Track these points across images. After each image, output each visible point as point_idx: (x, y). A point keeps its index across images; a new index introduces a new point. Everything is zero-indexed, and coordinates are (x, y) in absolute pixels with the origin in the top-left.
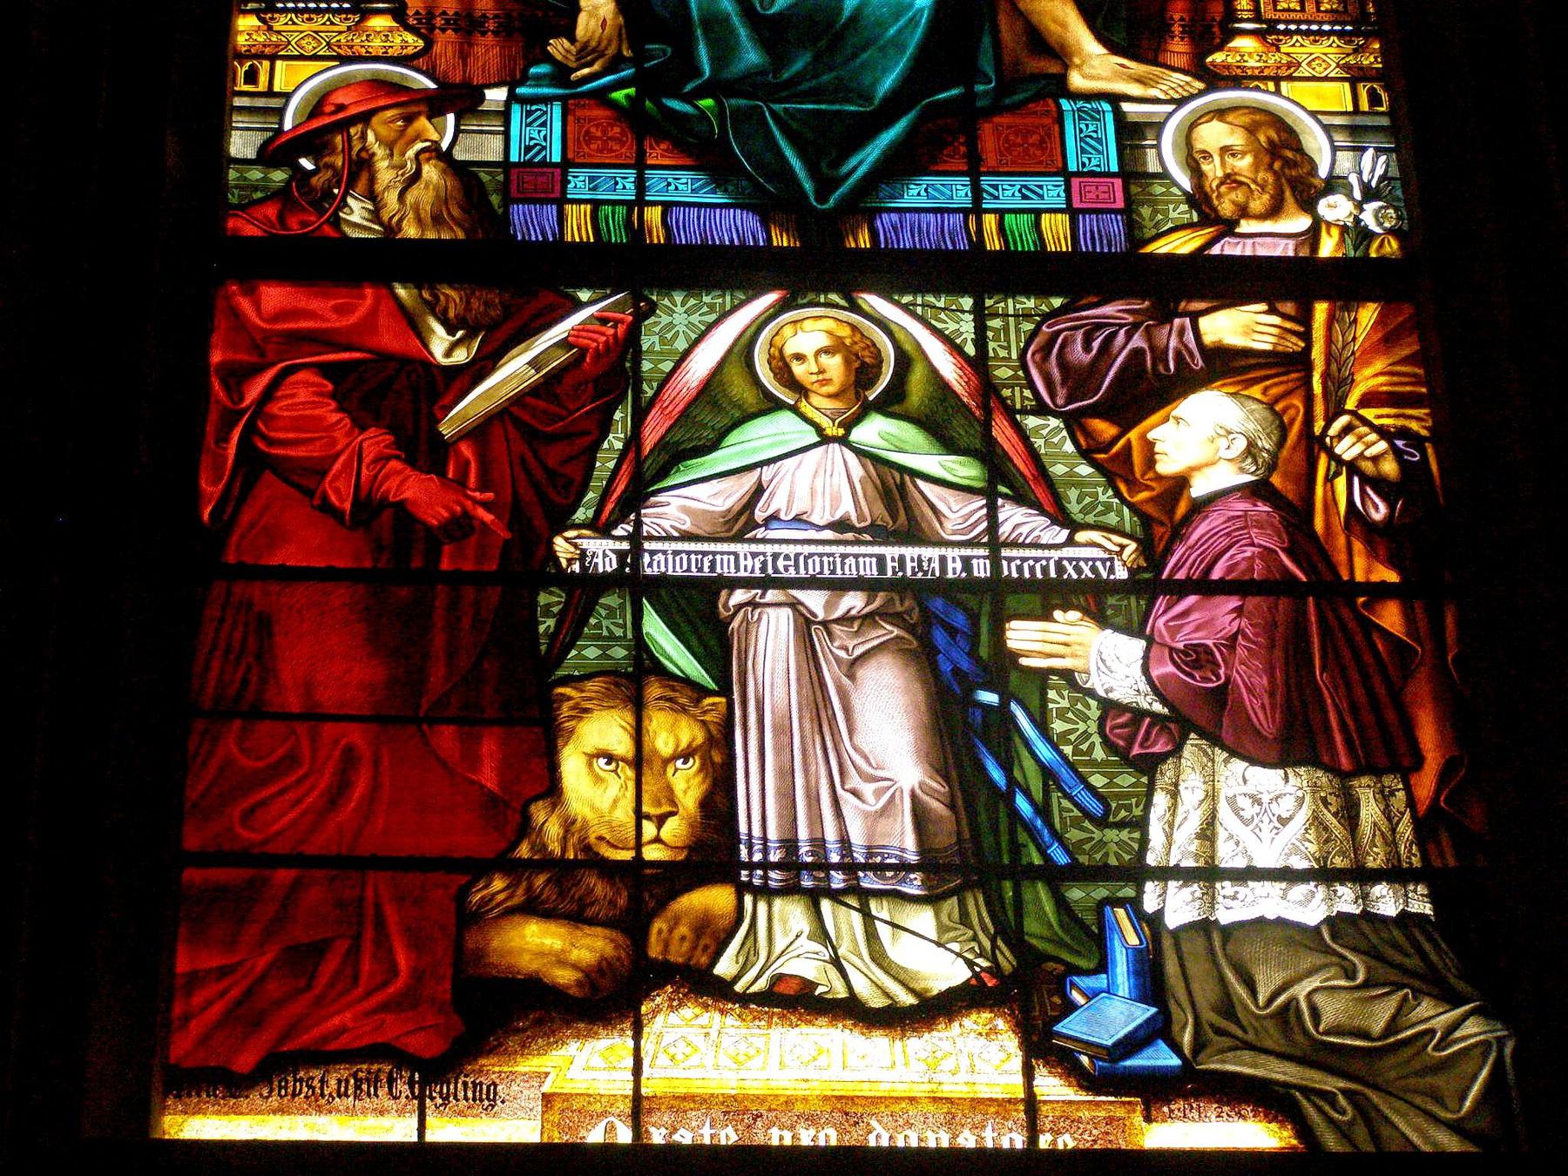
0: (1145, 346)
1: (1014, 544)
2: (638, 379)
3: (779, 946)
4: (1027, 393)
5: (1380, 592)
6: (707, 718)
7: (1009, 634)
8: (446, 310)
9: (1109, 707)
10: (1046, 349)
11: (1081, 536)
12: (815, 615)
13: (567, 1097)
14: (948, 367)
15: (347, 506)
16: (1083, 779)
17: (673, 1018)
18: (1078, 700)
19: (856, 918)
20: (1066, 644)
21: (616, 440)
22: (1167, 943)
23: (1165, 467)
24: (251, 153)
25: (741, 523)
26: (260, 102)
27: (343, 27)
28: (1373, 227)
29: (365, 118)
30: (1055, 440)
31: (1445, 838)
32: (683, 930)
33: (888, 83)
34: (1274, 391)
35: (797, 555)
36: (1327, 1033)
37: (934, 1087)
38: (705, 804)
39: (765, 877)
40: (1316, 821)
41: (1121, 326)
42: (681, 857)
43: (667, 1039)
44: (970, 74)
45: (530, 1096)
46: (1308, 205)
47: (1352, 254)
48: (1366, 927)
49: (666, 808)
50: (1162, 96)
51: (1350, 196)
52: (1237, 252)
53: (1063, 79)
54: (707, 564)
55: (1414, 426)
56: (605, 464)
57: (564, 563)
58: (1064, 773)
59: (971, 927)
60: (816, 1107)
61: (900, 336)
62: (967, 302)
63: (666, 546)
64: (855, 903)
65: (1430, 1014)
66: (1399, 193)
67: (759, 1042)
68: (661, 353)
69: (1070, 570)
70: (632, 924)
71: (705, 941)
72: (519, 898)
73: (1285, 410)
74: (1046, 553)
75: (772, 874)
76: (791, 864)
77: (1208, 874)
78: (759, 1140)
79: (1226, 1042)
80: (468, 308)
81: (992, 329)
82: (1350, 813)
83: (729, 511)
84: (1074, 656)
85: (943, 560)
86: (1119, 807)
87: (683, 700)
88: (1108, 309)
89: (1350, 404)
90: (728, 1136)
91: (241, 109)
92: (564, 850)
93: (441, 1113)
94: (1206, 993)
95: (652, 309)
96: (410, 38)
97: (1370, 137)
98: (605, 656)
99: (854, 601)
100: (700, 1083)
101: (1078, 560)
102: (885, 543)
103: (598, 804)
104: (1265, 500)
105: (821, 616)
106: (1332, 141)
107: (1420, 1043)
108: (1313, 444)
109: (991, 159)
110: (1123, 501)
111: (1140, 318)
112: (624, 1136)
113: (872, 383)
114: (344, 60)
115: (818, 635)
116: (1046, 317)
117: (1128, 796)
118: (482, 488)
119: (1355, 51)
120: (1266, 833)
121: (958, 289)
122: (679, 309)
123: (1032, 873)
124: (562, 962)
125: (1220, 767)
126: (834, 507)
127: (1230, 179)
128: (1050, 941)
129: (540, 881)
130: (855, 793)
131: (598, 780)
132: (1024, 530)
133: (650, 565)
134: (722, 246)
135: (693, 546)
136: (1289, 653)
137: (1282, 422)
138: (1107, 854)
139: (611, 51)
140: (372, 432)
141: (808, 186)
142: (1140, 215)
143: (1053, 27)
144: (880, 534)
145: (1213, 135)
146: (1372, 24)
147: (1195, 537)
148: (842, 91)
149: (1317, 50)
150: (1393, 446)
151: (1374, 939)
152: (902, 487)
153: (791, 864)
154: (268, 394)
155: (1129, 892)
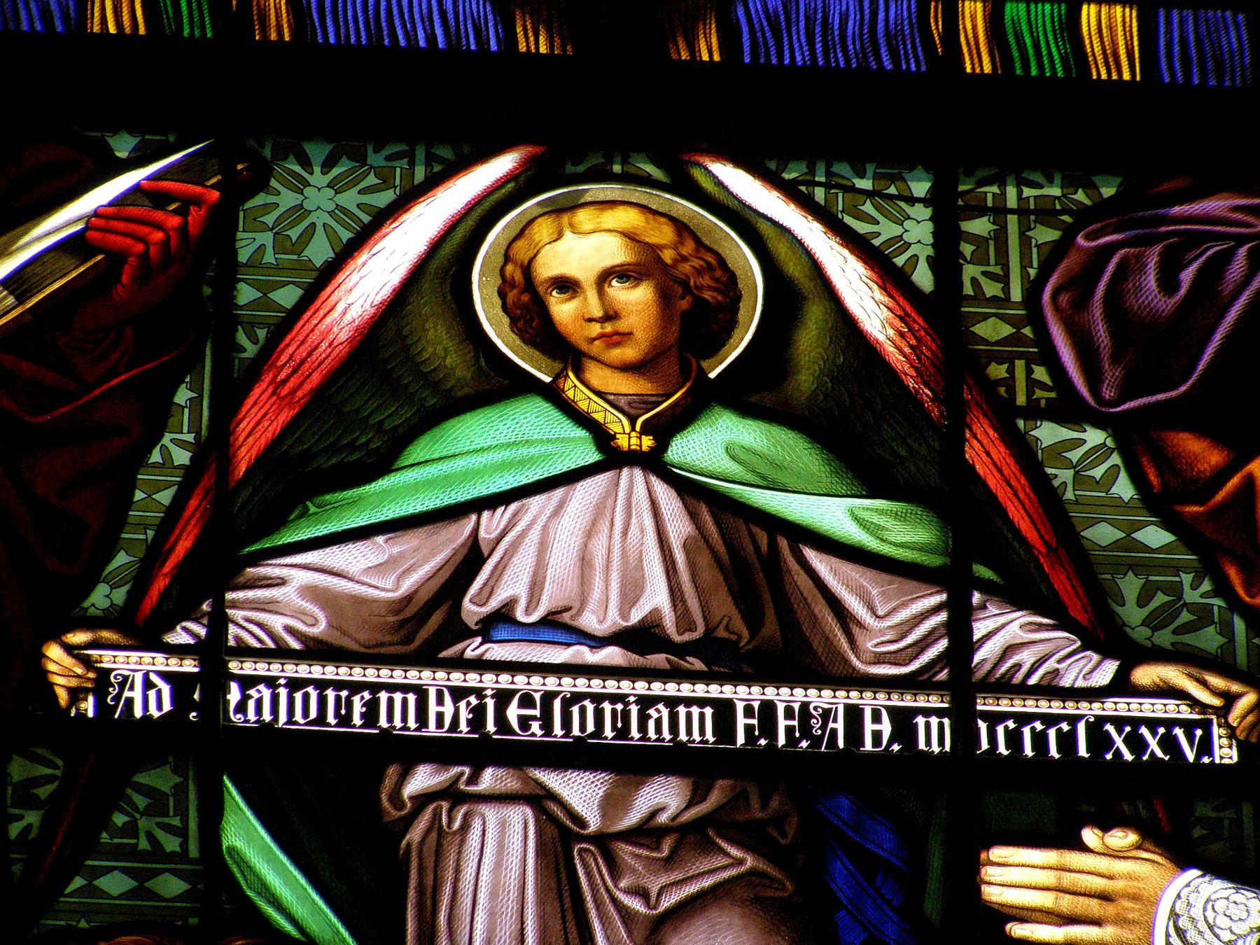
1: (1005, 686)
2: (225, 317)
4: (1040, 373)
7: (989, 873)
10: (1081, 284)
11: (1145, 675)
12: (582, 823)
20: (1105, 897)
25: (431, 627)
30: (1098, 472)
35: (548, 697)
41: (1241, 240)
54: (358, 708)
56: (153, 496)
61: (781, 249)
68: (277, 268)
69: (1119, 742)
74: (1071, 708)
83: (408, 599)
84: (1120, 921)
85: (854, 715)
88: (1216, 205)
98: (140, 892)
99: (662, 797)
101: (1136, 722)
102: (736, 678)
105: (594, 821)
110: (1235, 604)
115: (588, 870)
116: (1083, 217)
132: (1026, 657)
133: (241, 708)
144: (722, 659)
152: (773, 562)
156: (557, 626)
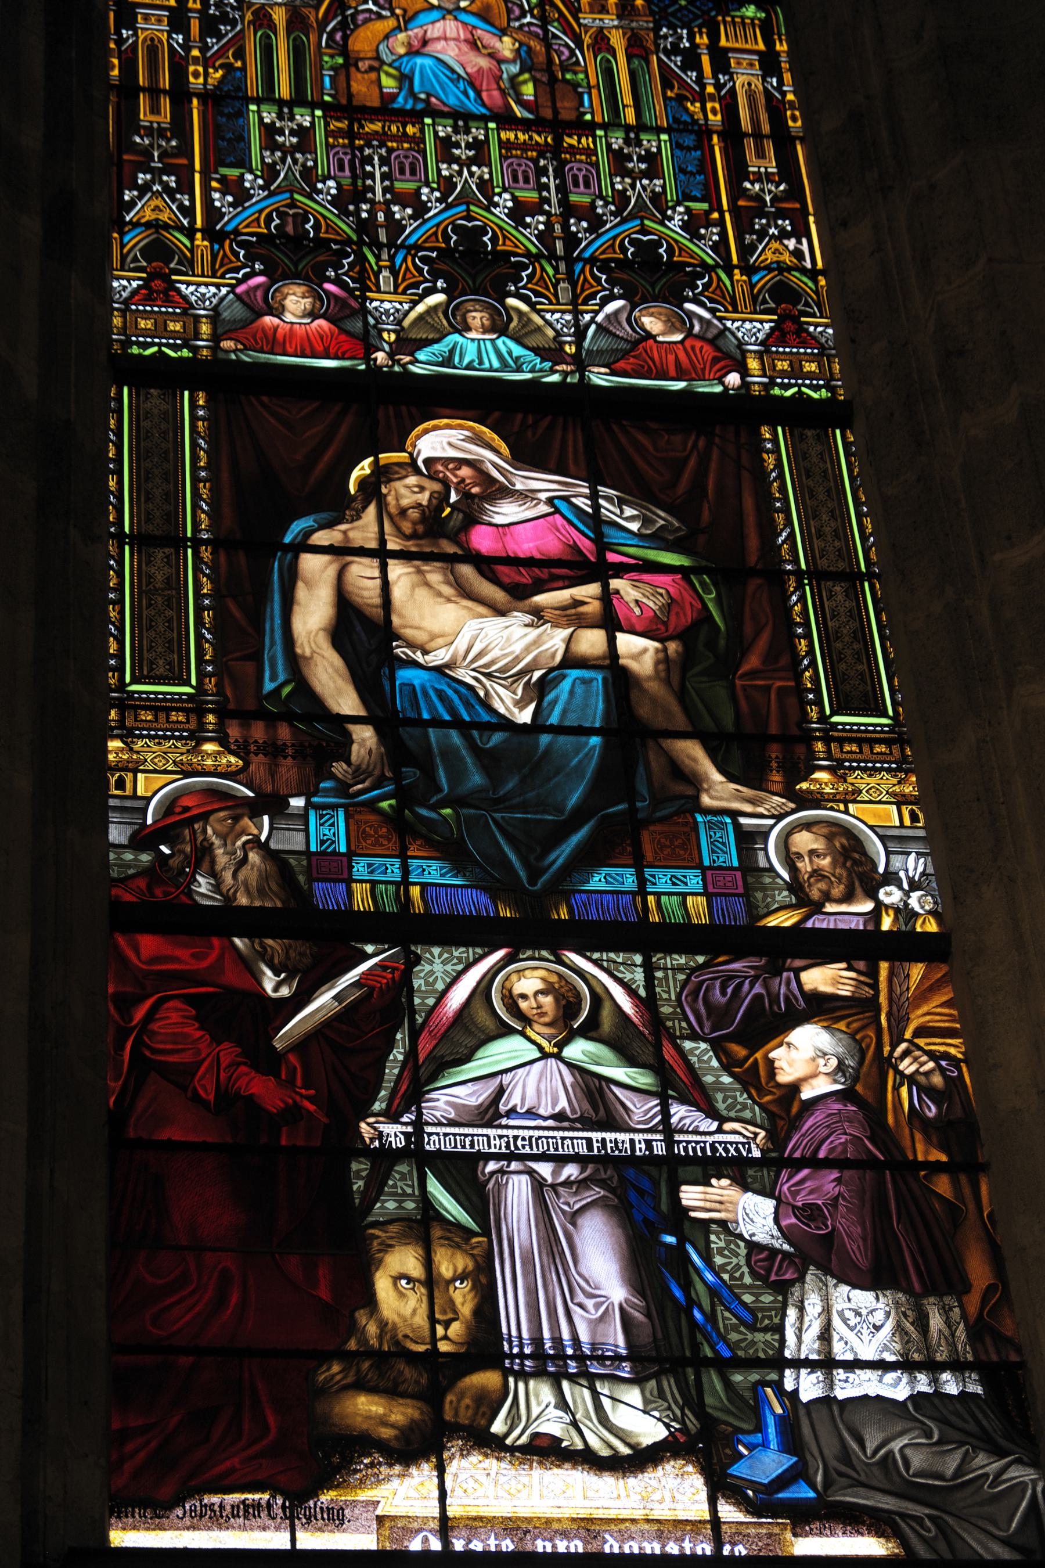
0: (763, 992)
1: (681, 1131)
2: (413, 1011)
3: (535, 1413)
4: (684, 1024)
5: (936, 1167)
6: (475, 1252)
7: (682, 1195)
8: (272, 957)
9: (753, 1246)
11: (728, 1126)
12: (545, 1180)
13: (394, 1518)
14: (626, 1005)
15: (211, 1097)
16: (738, 1297)
17: (464, 1463)
18: (731, 1242)
19: (587, 1393)
20: (721, 1203)
21: (398, 1054)
22: (802, 1412)
23: (783, 1078)
24: (124, 841)
25: (489, 1114)
26: (128, 804)
27: (184, 749)
28: (917, 909)
29: (205, 817)
30: (705, 1058)
31: (988, 1340)
32: (467, 1401)
33: (574, 800)
34: (855, 1025)
35: (531, 1138)
36: (915, 1475)
37: (647, 1512)
38: (477, 1312)
39: (522, 1365)
40: (899, 1328)
41: (746, 978)
42: (463, 1350)
43: (462, 1477)
44: (630, 795)
45: (368, 1518)
46: (873, 895)
47: (903, 928)
48: (936, 1401)
49: (450, 1316)
50: (766, 813)
51: (900, 887)
52: (824, 926)
53: (697, 798)
54: (468, 1143)
55: (952, 1051)
56: (391, 1071)
57: (368, 1141)
58: (725, 1293)
59: (666, 1401)
60: (566, 1525)
61: (593, 983)
62: (638, 959)
63: (438, 1130)
64: (585, 1383)
65: (985, 1464)
66: (934, 885)
67: (525, 1480)
68: (426, 992)
69: (721, 1150)
70: (432, 1397)
71: (483, 1409)
72: (350, 1380)
73: (863, 1038)
74: (703, 1138)
75: (527, 1363)
76: (539, 1355)
77: (827, 1364)
78: (529, 1548)
79: (844, 1481)
80: (288, 957)
81: (659, 979)
82: (922, 1323)
83: (481, 1105)
84: (727, 1211)
85: (632, 1141)
86: (764, 1317)
87: (457, 1239)
88: (736, 966)
89: (908, 1035)
90: (508, 1545)
91: (116, 809)
92: (381, 1344)
93: (306, 1530)
94: (831, 1449)
95: (418, 960)
96: (233, 759)
97: (913, 845)
99: (571, 1171)
100: (485, 1509)
101: (726, 1143)
102: (592, 1130)
103: (402, 1312)
104: (853, 1103)
105: (550, 1180)
106: (885, 848)
107: (980, 1482)
108: (885, 1064)
109: (649, 856)
110: (755, 1102)
111: (759, 972)
112: (436, 1545)
113: (575, 1016)
114: (187, 775)
115: (549, 1196)
116: (693, 970)
117: (770, 1309)
118: (307, 1088)
119: (899, 783)
120: (866, 1337)
121: (629, 948)
122: (437, 961)
123: (707, 1363)
124: (383, 1422)
125: (831, 1290)
126: (555, 1103)
127: (817, 873)
128: (721, 1410)
129: (366, 1365)
130: (581, 1306)
131: (402, 1295)
132: (687, 1121)
133: (429, 1143)
134: (464, 916)
135: (456, 1130)
136: (877, 1211)
137: (861, 1048)
138: (757, 1350)
139: (377, 772)
140: (226, 1045)
141: (522, 873)
142: (755, 898)
143: (687, 761)
144: (588, 1124)
145: (804, 841)
146: (911, 763)
147: (805, 1127)
148: (541, 805)
149: (873, 781)
150: (939, 1066)
151: (945, 1412)
152: (601, 1091)
153: (539, 1355)
154: (150, 1017)
155: (773, 1376)
156: (531, 1114)
